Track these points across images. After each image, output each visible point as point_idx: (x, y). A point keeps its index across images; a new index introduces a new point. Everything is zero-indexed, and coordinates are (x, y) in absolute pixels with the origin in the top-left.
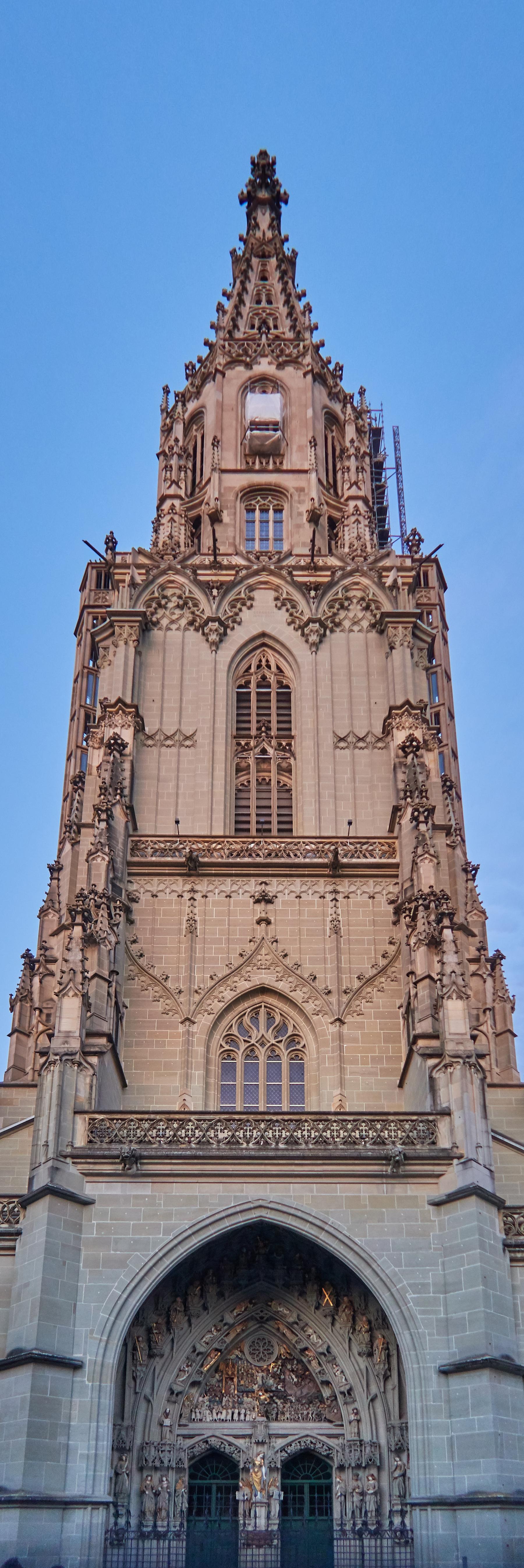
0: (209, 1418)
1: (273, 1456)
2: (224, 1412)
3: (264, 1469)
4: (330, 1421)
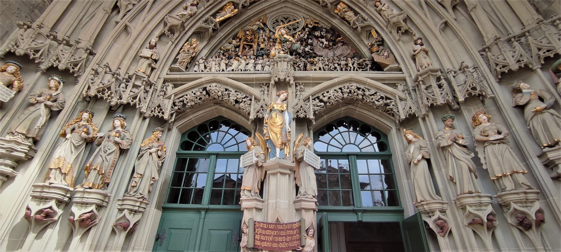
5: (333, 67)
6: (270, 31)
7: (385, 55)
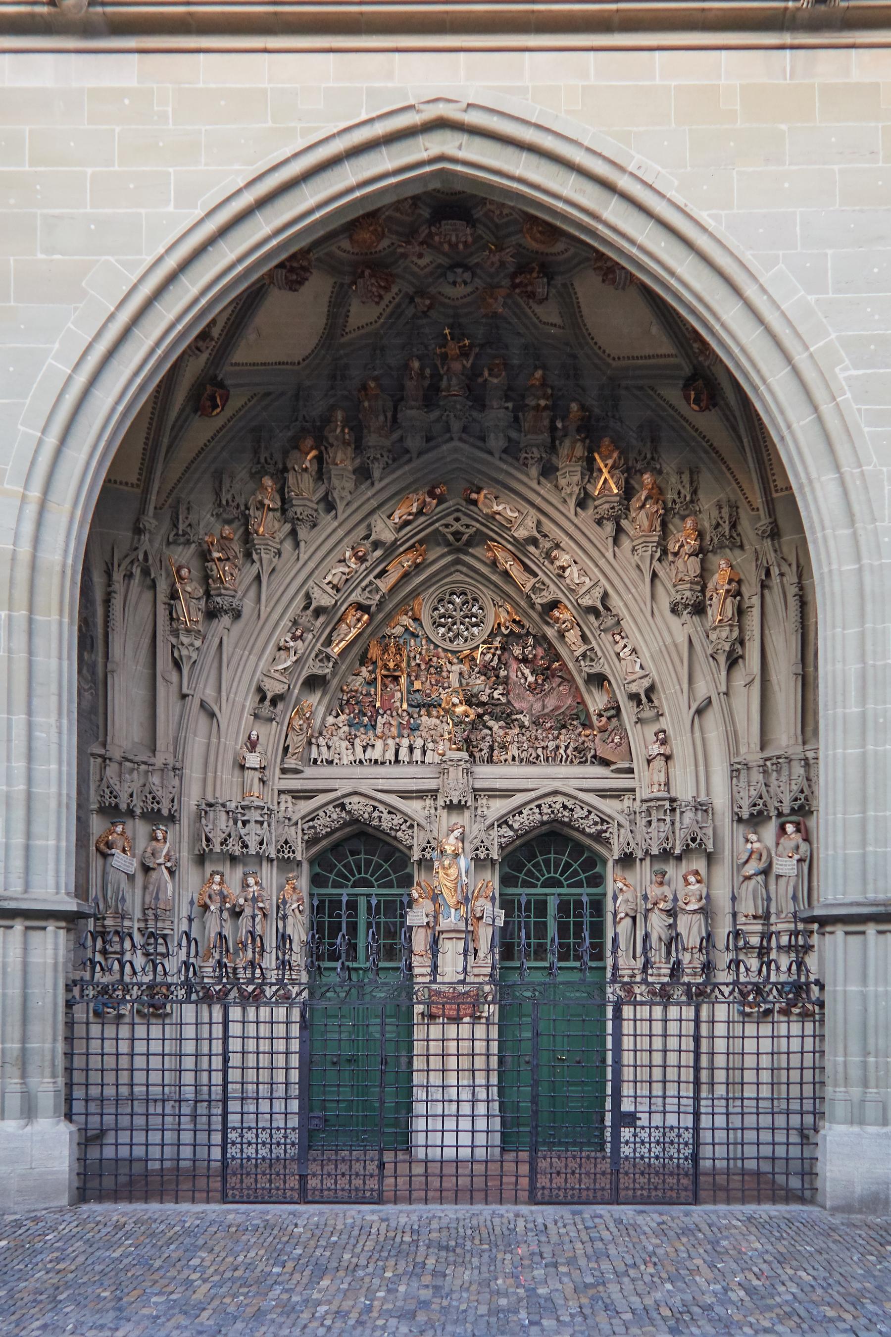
0: (347, 757)
1: (483, 836)
2: (379, 744)
3: (463, 862)
5: (534, 755)
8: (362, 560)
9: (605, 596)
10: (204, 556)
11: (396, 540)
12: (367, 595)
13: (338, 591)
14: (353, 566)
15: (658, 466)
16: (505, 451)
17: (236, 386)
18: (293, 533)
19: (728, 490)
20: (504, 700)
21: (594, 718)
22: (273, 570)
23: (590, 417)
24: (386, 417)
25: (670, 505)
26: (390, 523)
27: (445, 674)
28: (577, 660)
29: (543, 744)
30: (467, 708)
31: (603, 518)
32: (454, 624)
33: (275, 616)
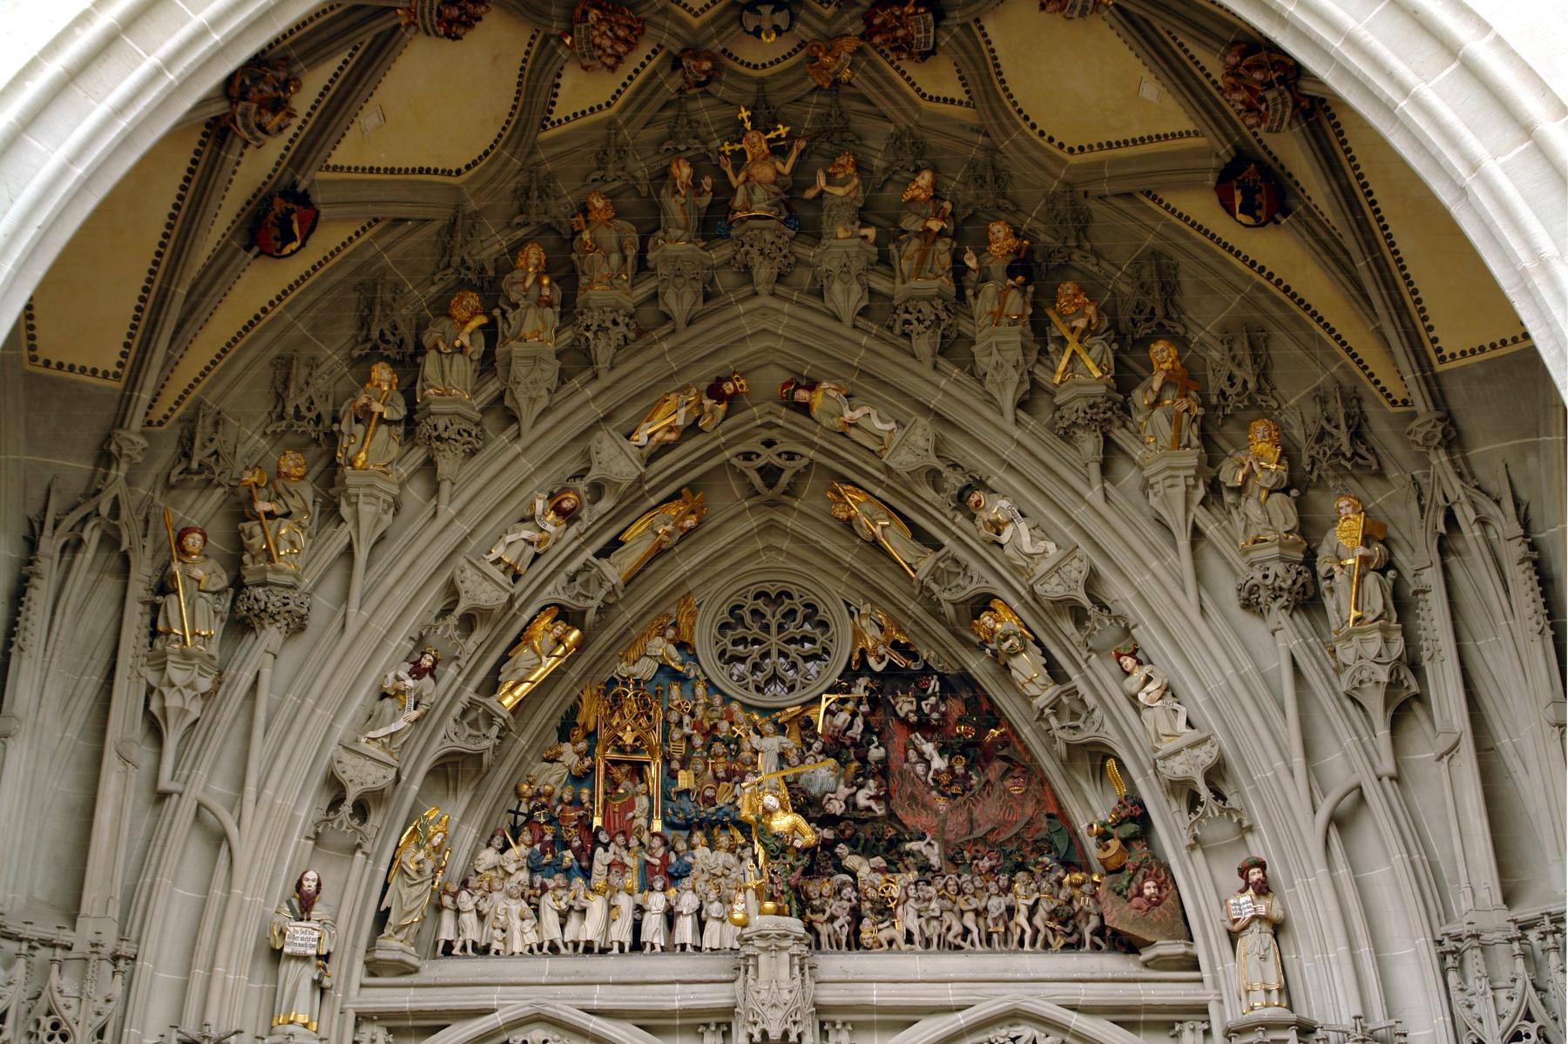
4: (1126, 945)
5: (957, 928)
6: (711, 686)
7: (1147, 892)
8: (568, 516)
9: (1092, 581)
10: (241, 510)
11: (641, 480)
12: (578, 589)
13: (516, 577)
14: (550, 528)
15: (1181, 330)
16: (864, 312)
17: (328, 204)
18: (430, 464)
19: (1334, 369)
20: (879, 810)
21: (1091, 844)
22: (382, 538)
23: (1030, 250)
24: (625, 259)
25: (1214, 400)
26: (629, 446)
27: (746, 755)
28: (1041, 716)
29: (975, 903)
30: (800, 820)
31: (1074, 423)
32: (766, 655)
33: (379, 626)
